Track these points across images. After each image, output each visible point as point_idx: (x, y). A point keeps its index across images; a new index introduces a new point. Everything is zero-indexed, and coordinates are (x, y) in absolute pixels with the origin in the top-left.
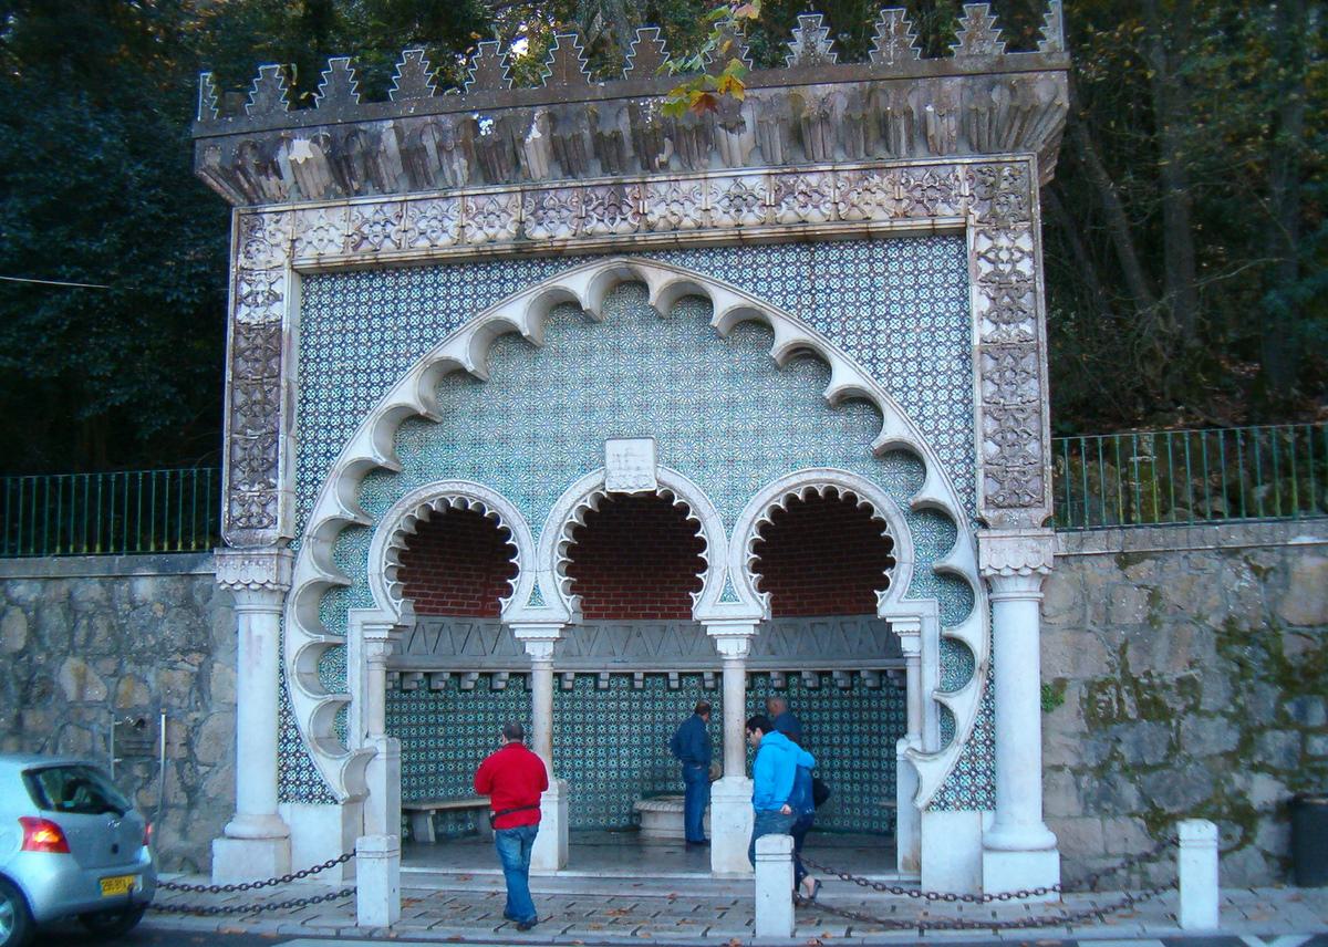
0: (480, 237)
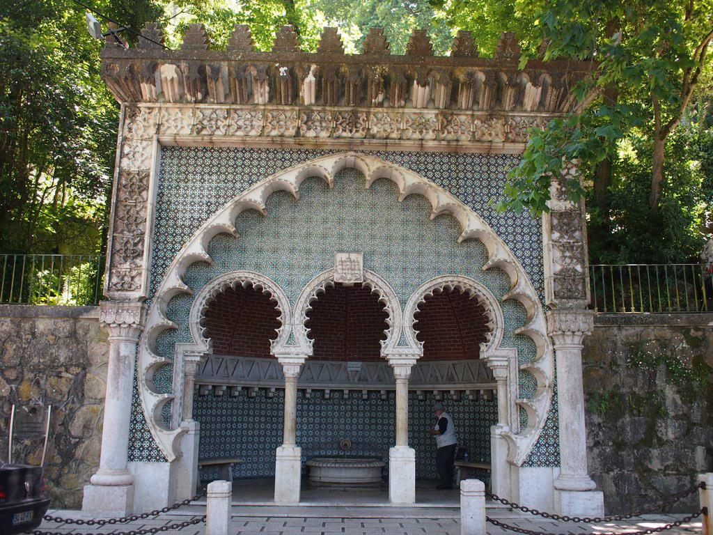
0: (274, 133)
